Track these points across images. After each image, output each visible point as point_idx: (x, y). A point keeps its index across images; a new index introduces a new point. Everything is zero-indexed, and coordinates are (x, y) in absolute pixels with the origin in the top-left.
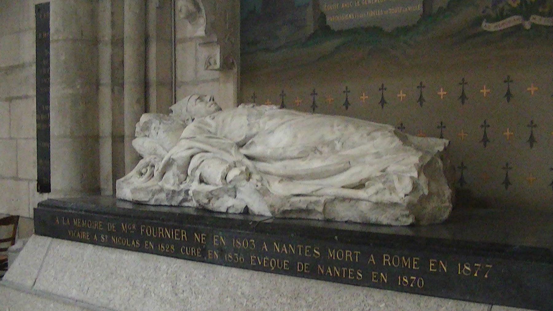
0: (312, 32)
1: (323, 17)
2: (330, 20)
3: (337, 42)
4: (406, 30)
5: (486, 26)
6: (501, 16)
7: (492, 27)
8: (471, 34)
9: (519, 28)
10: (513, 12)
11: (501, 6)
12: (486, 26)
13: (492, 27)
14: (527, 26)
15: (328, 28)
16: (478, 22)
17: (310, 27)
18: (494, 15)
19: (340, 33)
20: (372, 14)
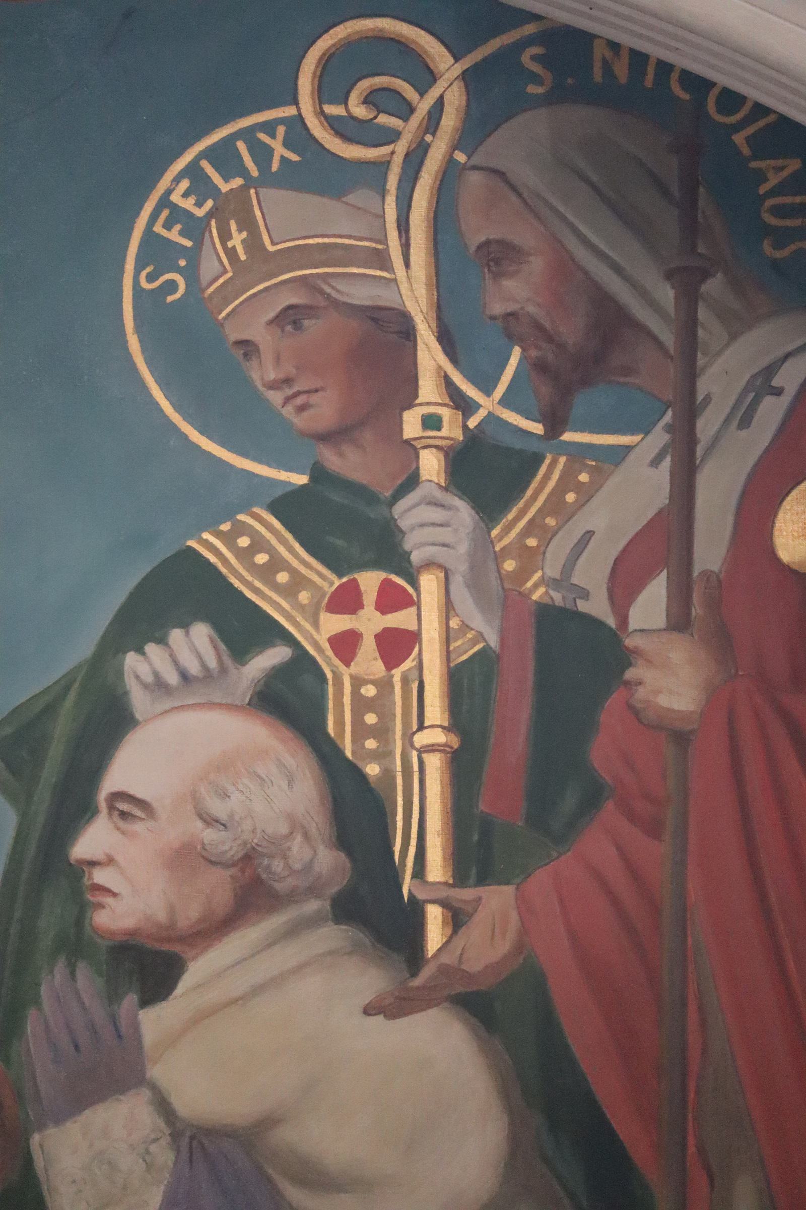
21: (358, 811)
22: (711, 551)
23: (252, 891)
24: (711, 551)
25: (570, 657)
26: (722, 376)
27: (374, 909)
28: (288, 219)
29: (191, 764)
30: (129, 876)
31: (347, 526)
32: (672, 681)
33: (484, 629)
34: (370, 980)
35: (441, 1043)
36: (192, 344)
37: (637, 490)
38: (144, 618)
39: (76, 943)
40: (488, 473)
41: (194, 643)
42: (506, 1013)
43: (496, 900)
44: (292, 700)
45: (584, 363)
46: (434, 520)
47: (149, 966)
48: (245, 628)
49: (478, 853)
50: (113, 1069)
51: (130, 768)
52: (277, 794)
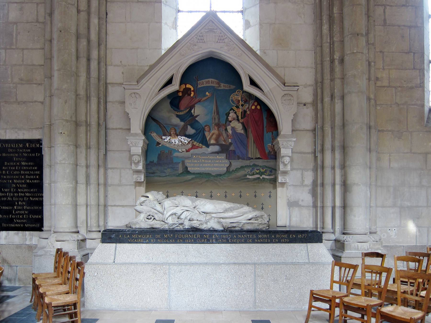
0: (182, 172)
1: (187, 168)
2: (189, 169)
3: (193, 176)
4: (220, 175)
5: (248, 176)
6: (253, 174)
7: (250, 177)
8: (243, 179)
9: (259, 178)
10: (257, 174)
11: (253, 171)
12: (248, 176)
13: (250, 177)
14: (261, 178)
15: (189, 171)
16: (246, 175)
17: (181, 170)
18: (251, 174)
19: (194, 174)
20: (207, 169)
21: (238, 117)
22: (250, 108)
23: (234, 119)
24: (250, 108)
25: (245, 112)
26: (250, 102)
27: (238, 120)
28: (236, 96)
29: (232, 115)
30: (230, 119)
31: (237, 107)
32: (248, 112)
33: (242, 111)
34: (238, 122)
35: (240, 124)
36: (232, 101)
37: (247, 106)
38: (231, 110)
39: (228, 121)
40: (242, 105)
41: (232, 111)
42: (242, 123)
43: (242, 120)
44: (235, 113)
45: (246, 102)
46: (240, 107)
47: (231, 122)
48: (234, 110)
49: (242, 118)
50: (229, 125)
51: (230, 115)
52: (235, 116)
